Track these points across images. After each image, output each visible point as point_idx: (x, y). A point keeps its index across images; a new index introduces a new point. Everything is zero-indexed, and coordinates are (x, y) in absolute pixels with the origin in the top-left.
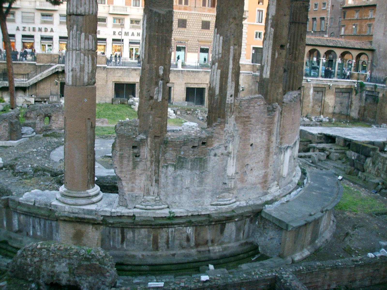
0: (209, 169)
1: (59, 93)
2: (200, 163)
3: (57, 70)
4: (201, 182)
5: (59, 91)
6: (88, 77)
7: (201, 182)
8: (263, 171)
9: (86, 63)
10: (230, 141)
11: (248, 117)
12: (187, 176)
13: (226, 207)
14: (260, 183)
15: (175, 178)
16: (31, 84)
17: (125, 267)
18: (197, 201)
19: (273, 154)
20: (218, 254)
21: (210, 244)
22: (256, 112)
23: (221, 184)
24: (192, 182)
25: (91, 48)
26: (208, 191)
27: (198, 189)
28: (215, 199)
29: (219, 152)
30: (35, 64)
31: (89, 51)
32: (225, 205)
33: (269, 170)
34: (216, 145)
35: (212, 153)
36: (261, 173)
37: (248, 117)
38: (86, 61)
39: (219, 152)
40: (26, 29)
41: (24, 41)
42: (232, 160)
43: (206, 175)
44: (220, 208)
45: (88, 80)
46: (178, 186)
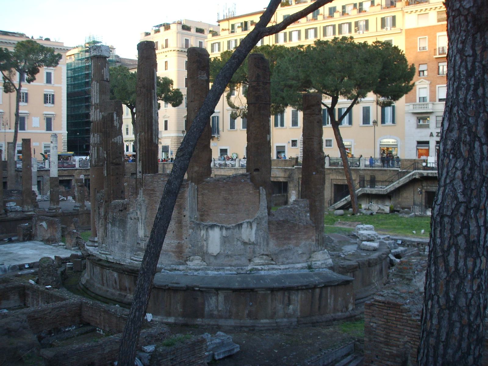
0: (128, 229)
1: (424, 204)
2: (123, 223)
3: (414, 177)
4: (124, 239)
5: (424, 201)
6: (95, 161)
7: (124, 239)
8: (176, 241)
9: (93, 152)
10: (138, 208)
11: (153, 190)
12: (115, 231)
13: (137, 262)
14: (173, 252)
15: (112, 232)
16: (389, 191)
17: (89, 292)
18: (122, 253)
19: (188, 227)
20: (129, 301)
21: (128, 291)
22: (160, 186)
23: (135, 244)
24: (119, 237)
25: (96, 142)
26: (128, 247)
27: (123, 243)
28: (132, 255)
29: (133, 216)
30: (398, 170)
31: (95, 144)
32: (136, 261)
33: (183, 242)
34: (131, 210)
35: (129, 216)
36: (172, 242)
37: (153, 190)
38: (93, 150)
39: (133, 216)
40: (436, 134)
41: (418, 148)
42: (141, 224)
43: (126, 234)
44: (132, 262)
45: (95, 162)
46: (113, 239)
